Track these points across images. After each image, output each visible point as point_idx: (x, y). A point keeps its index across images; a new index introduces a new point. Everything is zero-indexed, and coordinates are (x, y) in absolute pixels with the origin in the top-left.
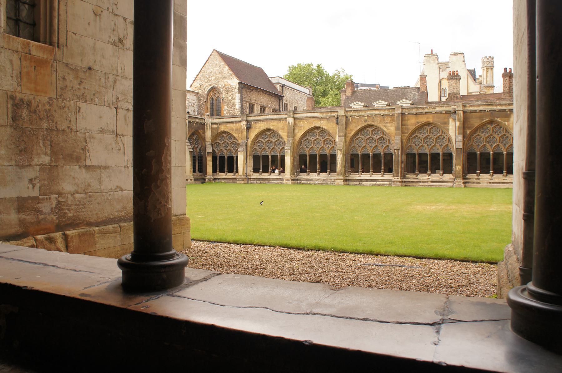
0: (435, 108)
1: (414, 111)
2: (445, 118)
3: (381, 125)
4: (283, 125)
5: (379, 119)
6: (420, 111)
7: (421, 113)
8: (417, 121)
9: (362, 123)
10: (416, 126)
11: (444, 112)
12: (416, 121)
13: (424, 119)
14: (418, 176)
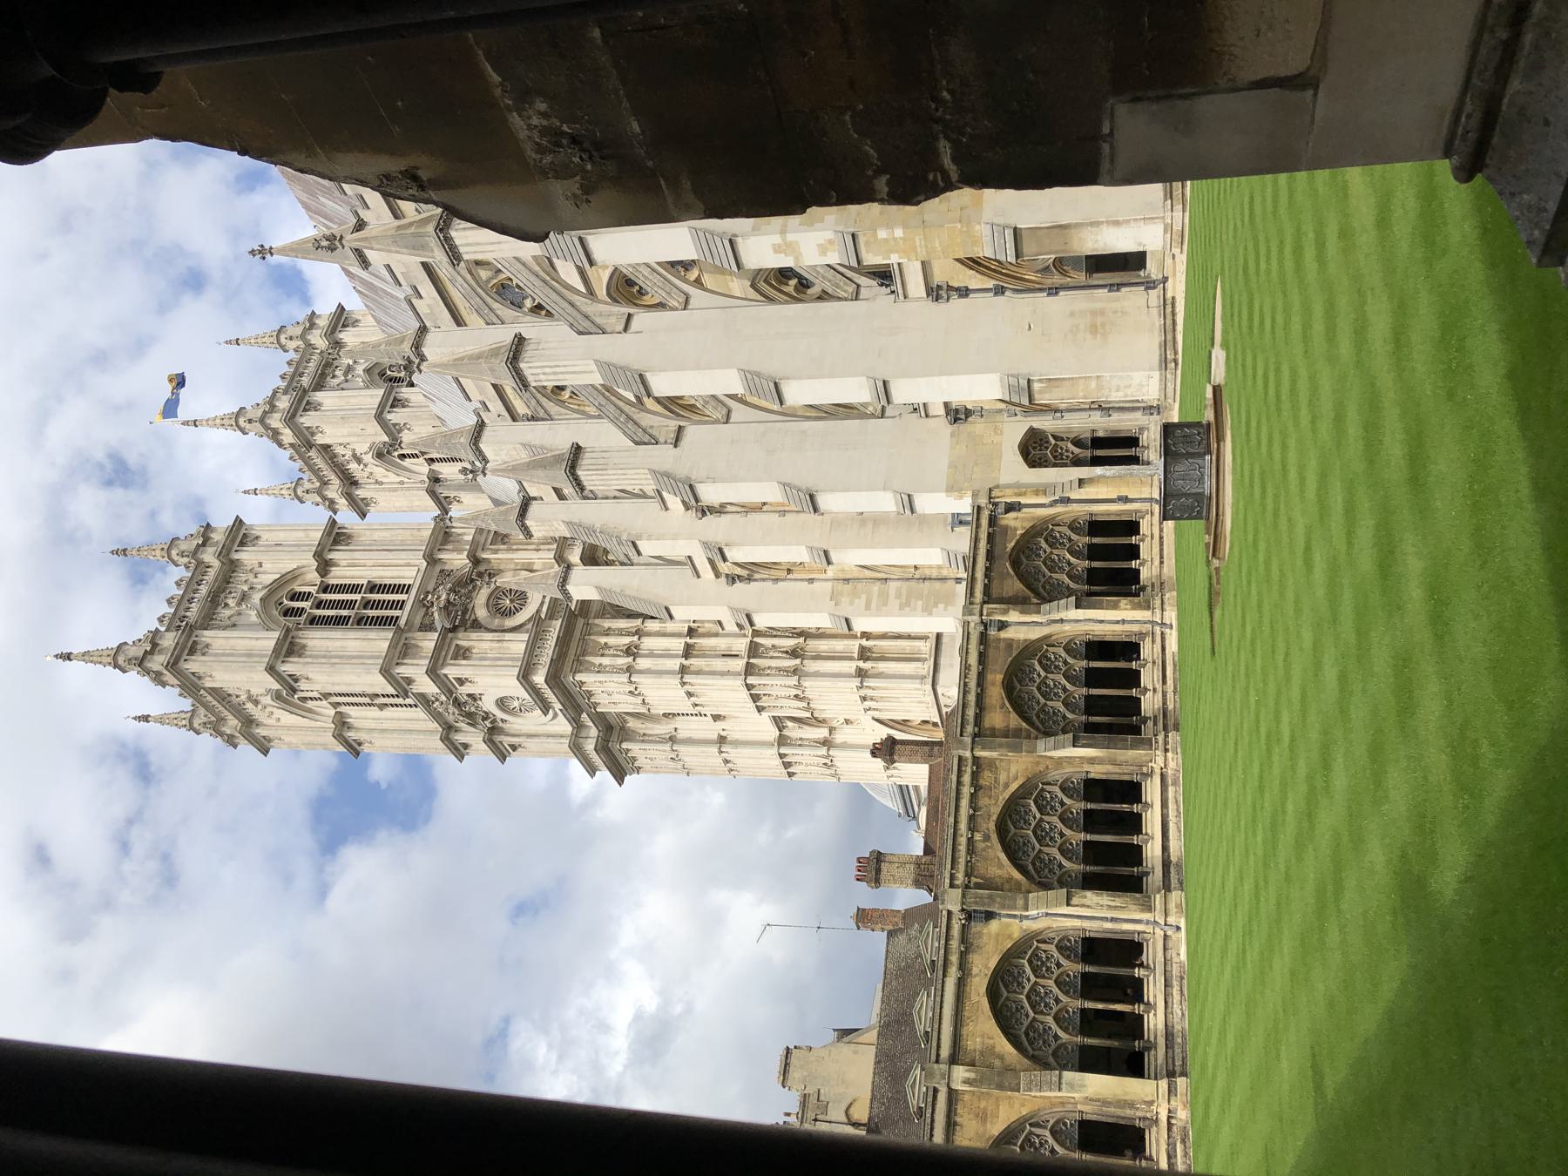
0: (970, 665)
1: (971, 712)
2: (997, 648)
3: (1001, 798)
4: (972, 1116)
5: (983, 801)
6: (972, 698)
7: (980, 698)
8: (998, 707)
9: (991, 847)
10: (1011, 710)
11: (982, 647)
12: (998, 710)
13: (995, 693)
14: (1149, 714)
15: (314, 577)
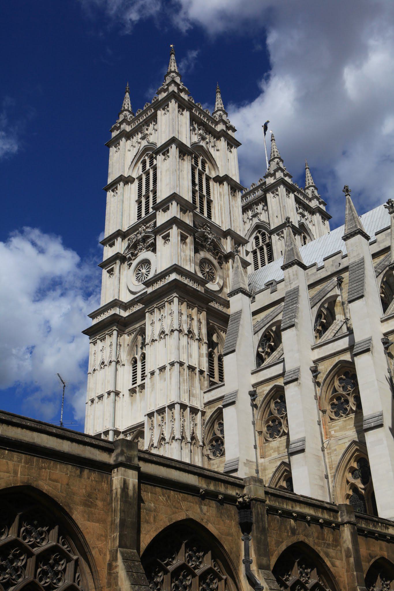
15: (213, 175)
